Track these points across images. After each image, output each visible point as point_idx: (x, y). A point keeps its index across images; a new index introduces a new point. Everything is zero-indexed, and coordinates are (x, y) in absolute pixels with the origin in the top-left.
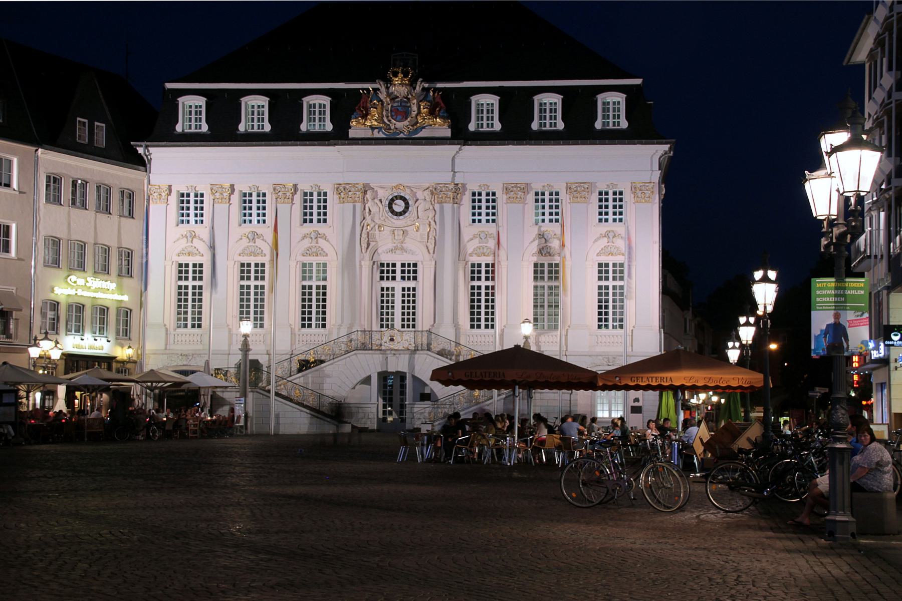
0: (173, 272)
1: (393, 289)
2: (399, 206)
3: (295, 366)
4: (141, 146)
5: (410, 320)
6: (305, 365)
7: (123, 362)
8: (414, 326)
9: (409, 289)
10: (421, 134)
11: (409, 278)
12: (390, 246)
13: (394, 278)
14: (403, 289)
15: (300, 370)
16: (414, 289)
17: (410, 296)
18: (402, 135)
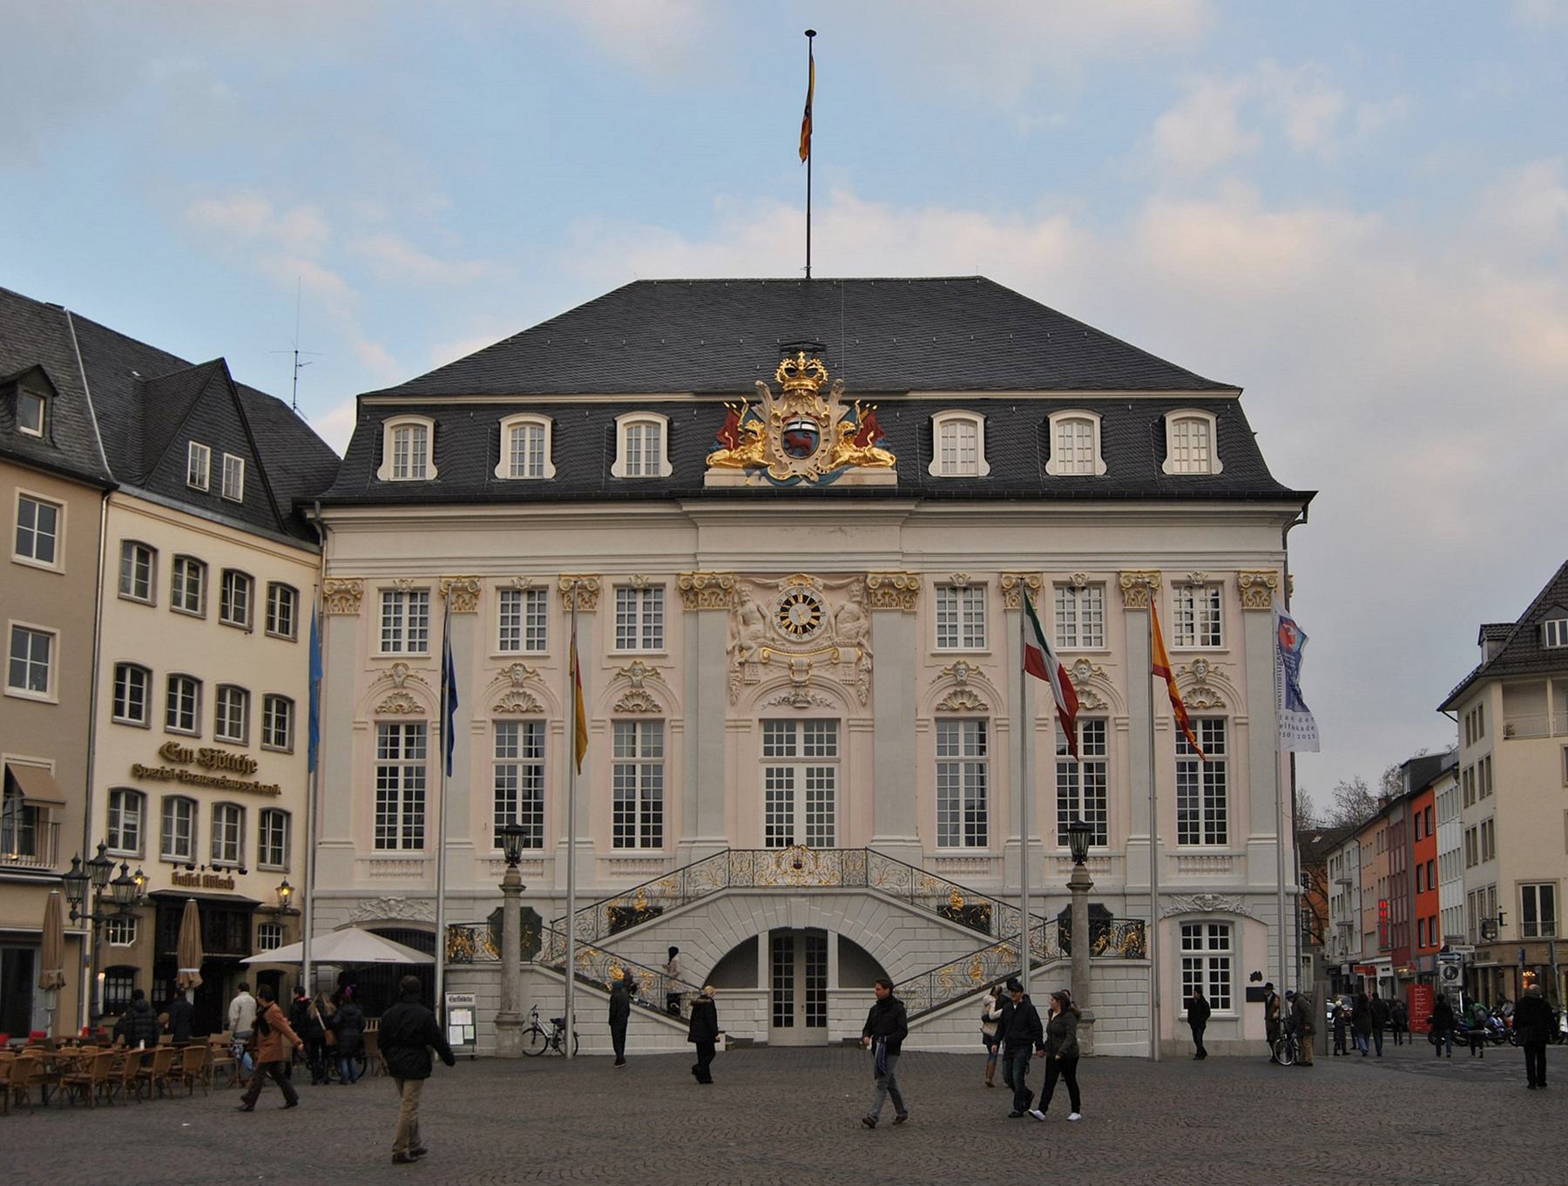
0: (370, 743)
1: (790, 772)
2: (800, 614)
3: (605, 921)
4: (311, 505)
5: (821, 835)
6: (624, 919)
7: (271, 912)
8: (831, 842)
9: (820, 771)
10: (839, 482)
11: (820, 752)
12: (783, 693)
13: (792, 751)
14: (810, 772)
15: (614, 929)
16: (831, 772)
17: (822, 787)
18: (804, 484)
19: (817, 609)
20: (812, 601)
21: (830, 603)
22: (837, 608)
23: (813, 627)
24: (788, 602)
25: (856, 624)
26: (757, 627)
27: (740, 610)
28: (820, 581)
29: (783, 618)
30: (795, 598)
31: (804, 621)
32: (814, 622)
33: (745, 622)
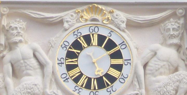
2: (94, 61)
19: (118, 55)
20: (111, 45)
21: (136, 47)
22: (147, 53)
23: (112, 79)
24: (77, 45)
25: (175, 76)
26: (33, 79)
27: (8, 56)
28: (122, 16)
29: (70, 68)
30: (88, 39)
31: (100, 71)
32: (114, 73)
33: (16, 73)
